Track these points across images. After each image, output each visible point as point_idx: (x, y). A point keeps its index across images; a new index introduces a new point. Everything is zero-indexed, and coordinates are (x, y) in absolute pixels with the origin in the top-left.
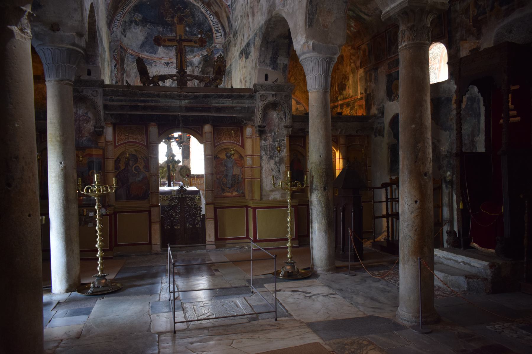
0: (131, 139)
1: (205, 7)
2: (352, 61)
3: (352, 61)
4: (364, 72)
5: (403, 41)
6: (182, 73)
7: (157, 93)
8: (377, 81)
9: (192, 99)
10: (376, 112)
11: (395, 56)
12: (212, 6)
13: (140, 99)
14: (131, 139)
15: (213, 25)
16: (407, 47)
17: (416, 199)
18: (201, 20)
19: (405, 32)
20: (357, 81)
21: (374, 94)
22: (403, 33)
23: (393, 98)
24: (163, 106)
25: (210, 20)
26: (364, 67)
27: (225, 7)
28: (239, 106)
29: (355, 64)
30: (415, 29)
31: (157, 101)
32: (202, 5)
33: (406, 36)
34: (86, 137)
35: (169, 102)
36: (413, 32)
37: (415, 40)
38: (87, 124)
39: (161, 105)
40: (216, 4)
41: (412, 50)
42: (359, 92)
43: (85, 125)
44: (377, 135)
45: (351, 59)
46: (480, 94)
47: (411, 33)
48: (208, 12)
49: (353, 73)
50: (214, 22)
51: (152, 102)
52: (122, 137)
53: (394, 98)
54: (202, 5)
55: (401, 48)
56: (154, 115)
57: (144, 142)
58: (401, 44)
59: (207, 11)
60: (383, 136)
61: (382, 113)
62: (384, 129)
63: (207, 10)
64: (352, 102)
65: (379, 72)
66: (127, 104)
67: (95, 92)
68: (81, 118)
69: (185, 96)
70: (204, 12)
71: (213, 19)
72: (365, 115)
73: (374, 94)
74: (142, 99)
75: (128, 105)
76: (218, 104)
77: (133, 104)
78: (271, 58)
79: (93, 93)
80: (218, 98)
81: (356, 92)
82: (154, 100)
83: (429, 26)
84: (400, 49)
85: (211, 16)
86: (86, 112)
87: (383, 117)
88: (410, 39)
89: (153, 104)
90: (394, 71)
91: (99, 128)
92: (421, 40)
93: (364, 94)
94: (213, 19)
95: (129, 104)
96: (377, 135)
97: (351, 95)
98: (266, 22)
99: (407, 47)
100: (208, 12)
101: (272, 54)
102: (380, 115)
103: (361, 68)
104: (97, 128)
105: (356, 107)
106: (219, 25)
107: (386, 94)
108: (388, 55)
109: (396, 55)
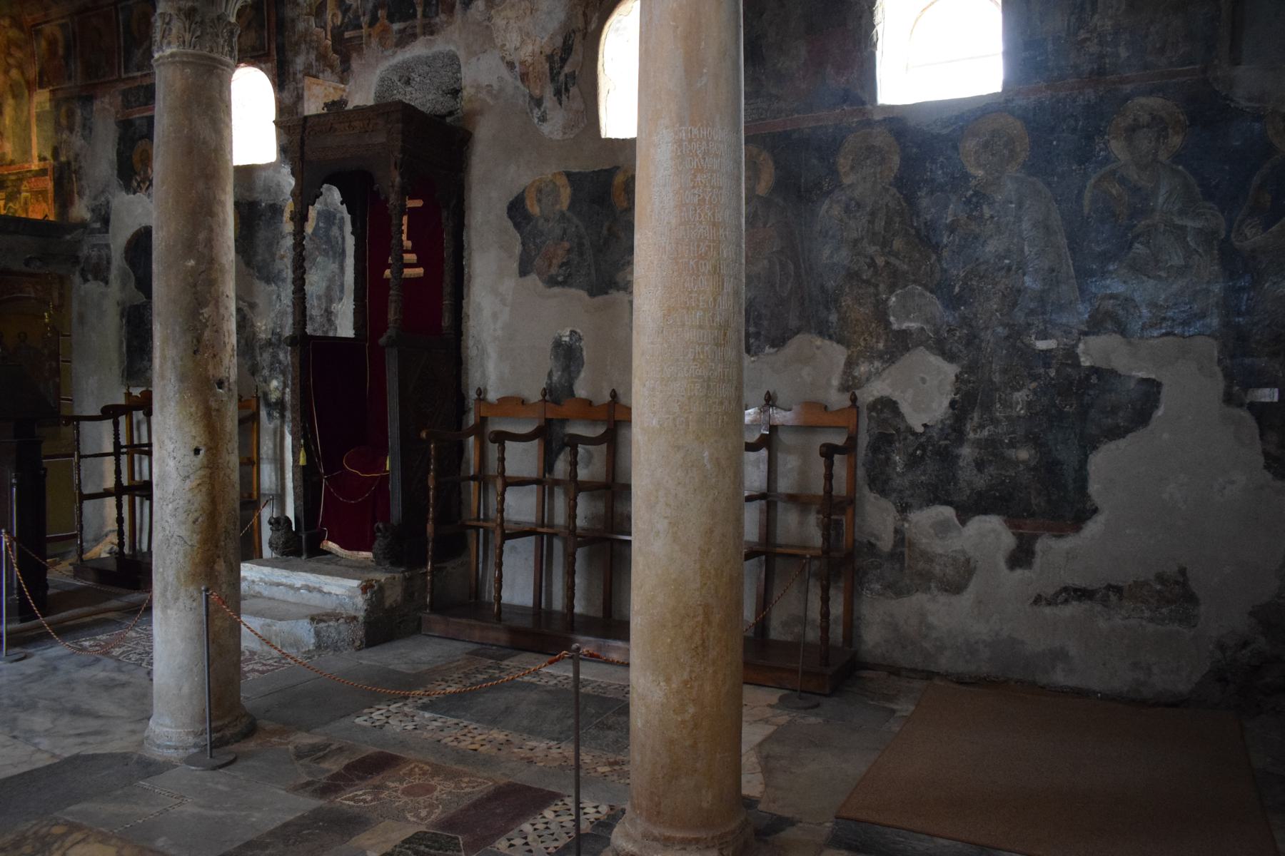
2: (11, 61)
3: (11, 61)
4: (50, 100)
5: (165, 41)
8: (91, 132)
10: (88, 216)
11: (141, 76)
16: (177, 59)
17: (196, 444)
19: (170, 20)
20: (28, 122)
22: (167, 20)
23: (135, 184)
26: (51, 88)
29: (23, 73)
30: (198, 19)
33: (174, 31)
36: (193, 26)
37: (198, 48)
41: (188, 70)
42: (35, 152)
44: (90, 277)
45: (10, 55)
46: (345, 205)
47: (187, 26)
49: (15, 97)
53: (139, 185)
55: (161, 57)
58: (160, 48)
60: (107, 283)
61: (106, 221)
62: (109, 263)
64: (13, 177)
65: (94, 109)
72: (52, 218)
81: (26, 152)
83: (233, 20)
84: (157, 60)
87: (107, 232)
88: (184, 42)
90: (137, 116)
92: (211, 51)
93: (52, 161)
96: (90, 277)
97: (9, 157)
99: (177, 59)
102: (98, 225)
103: (41, 86)
105: (24, 194)
107: (116, 172)
108: (123, 70)
109: (145, 75)
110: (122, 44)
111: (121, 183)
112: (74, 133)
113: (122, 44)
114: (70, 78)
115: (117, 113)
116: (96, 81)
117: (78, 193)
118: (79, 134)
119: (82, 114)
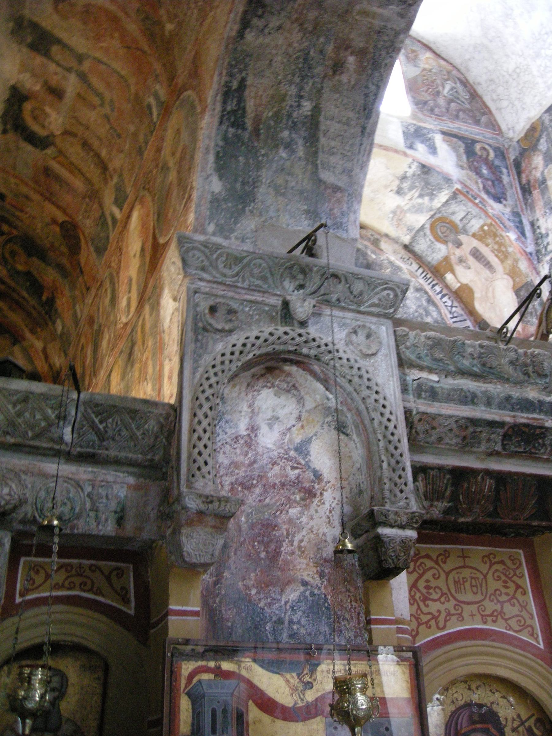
0: (472, 615)
1: (428, 276)
12: (453, 272)
14: (472, 615)
15: (454, 320)
18: (411, 311)
25: (444, 307)
27: (516, 261)
32: (421, 271)
34: (305, 584)
38: (306, 507)
40: (471, 261)
43: (294, 512)
48: (438, 289)
50: (455, 315)
52: (434, 607)
54: (421, 271)
57: (532, 634)
59: (434, 286)
63: (434, 282)
66: (497, 418)
67: (361, 338)
68: (273, 475)
70: (428, 288)
71: (452, 307)
75: (502, 424)
77: (523, 418)
79: (354, 337)
85: (445, 299)
86: (298, 440)
91: (402, 527)
94: (452, 307)
95: (508, 419)
100: (438, 289)
104: (392, 526)
106: (468, 323)
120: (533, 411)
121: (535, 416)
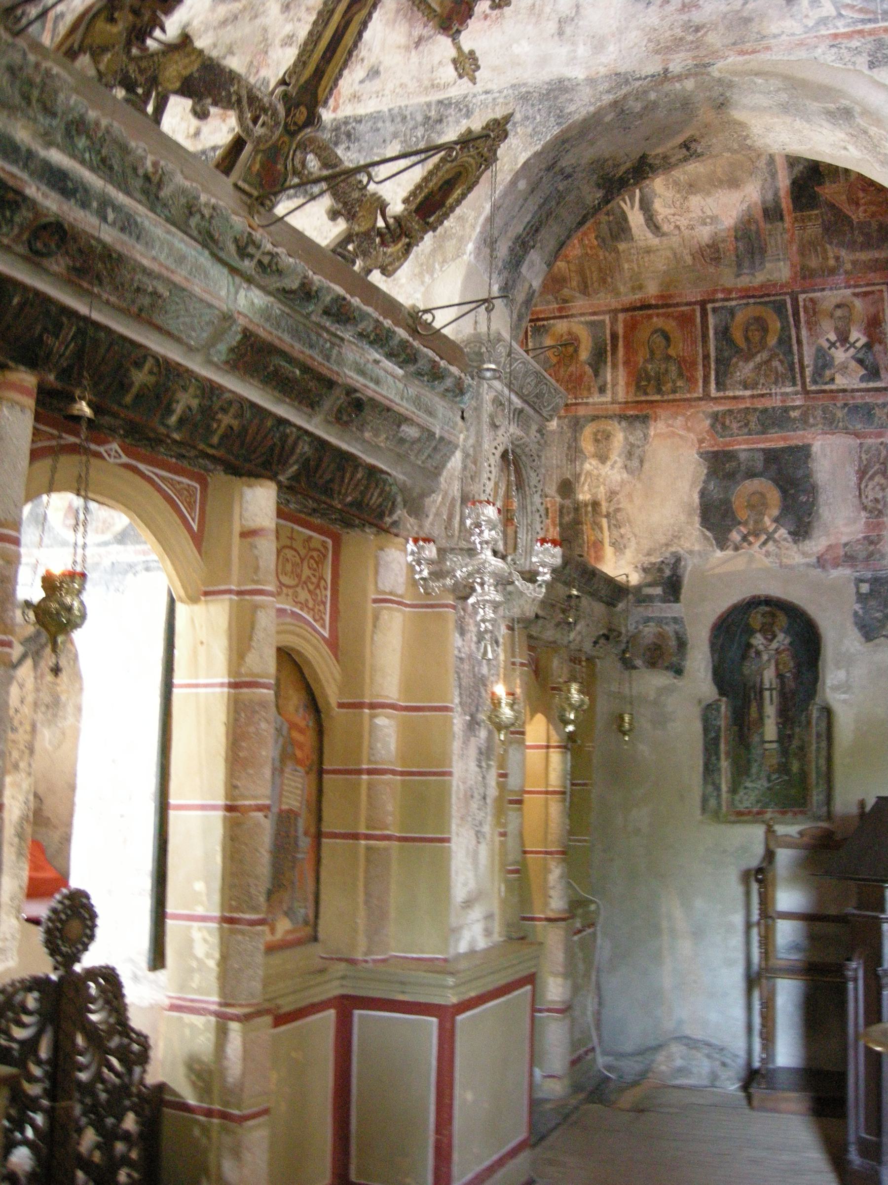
6: (302, 114)
7: (155, 164)
8: (642, 462)
9: (284, 294)
11: (752, 397)
13: (43, 153)
21: (618, 510)
24: (145, 271)
28: (420, 421)
31: (128, 225)
35: (181, 259)
39: (146, 262)
51: (104, 219)
53: (745, 538)
56: (73, 314)
60: (679, 671)
65: (652, 433)
69: (266, 260)
73: (618, 510)
74: (56, 157)
76: (361, 380)
78: (518, 237)
80: (371, 343)
82: (117, 208)
89: (108, 235)
90: (743, 447)
93: (558, 499)
96: (638, 662)
98: (621, 78)
101: (529, 223)
107: (697, 520)
108: (713, 386)
110: (713, 354)
111: (708, 534)
112: (609, 463)
113: (713, 354)
114: (602, 390)
115: (701, 441)
116: (658, 397)
117: (613, 544)
118: (619, 464)
119: (626, 439)
120: (15, 162)
121: (14, 170)
